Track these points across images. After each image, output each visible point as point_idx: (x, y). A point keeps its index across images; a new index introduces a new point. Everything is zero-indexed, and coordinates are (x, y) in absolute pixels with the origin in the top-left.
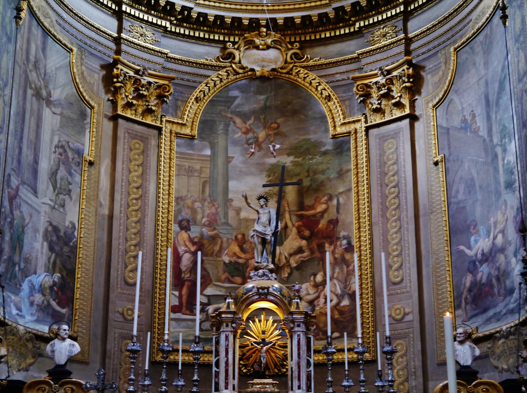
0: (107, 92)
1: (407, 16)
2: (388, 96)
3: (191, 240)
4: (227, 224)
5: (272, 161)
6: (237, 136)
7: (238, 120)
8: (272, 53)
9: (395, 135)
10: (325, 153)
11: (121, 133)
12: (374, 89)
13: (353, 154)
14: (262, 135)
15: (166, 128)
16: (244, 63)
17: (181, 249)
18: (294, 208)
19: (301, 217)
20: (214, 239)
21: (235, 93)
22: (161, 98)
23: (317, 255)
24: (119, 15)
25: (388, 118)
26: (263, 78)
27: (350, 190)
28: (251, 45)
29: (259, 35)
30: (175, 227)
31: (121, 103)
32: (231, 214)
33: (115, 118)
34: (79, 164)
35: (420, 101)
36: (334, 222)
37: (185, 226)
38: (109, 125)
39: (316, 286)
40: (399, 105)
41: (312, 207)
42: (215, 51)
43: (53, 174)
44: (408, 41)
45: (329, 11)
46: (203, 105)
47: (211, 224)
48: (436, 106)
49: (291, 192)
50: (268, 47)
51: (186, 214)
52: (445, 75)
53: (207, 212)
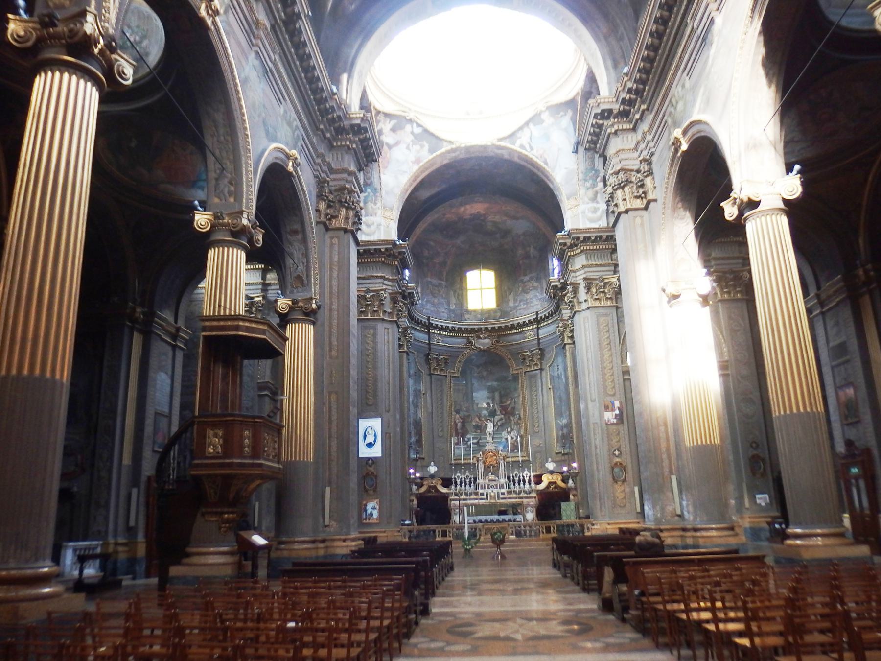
0: (427, 364)
1: (538, 328)
2: (532, 360)
3: (460, 417)
4: (473, 410)
5: (489, 384)
6: (476, 374)
7: (475, 368)
8: (487, 341)
9: (535, 376)
10: (509, 381)
11: (433, 380)
12: (527, 357)
13: (520, 381)
14: (485, 373)
15: (448, 375)
16: (476, 345)
17: (457, 421)
18: (498, 403)
19: (501, 406)
20: (469, 416)
21: (474, 357)
22: (446, 363)
23: (508, 421)
24: (429, 333)
25: (532, 369)
26: (484, 351)
27: (519, 396)
28: (479, 338)
29: (482, 334)
30: (454, 413)
31: (432, 368)
32: (475, 407)
33: (430, 374)
34: (420, 395)
35: (544, 363)
36: (514, 408)
37: (458, 412)
38: (428, 377)
39: (508, 433)
40: (536, 364)
41: (505, 402)
42: (465, 340)
43: (413, 401)
44: (539, 339)
45: (509, 324)
46: (462, 364)
47: (467, 411)
48: (549, 366)
49: (497, 395)
50: (485, 338)
51: (458, 408)
52: (552, 356)
53: (466, 405)
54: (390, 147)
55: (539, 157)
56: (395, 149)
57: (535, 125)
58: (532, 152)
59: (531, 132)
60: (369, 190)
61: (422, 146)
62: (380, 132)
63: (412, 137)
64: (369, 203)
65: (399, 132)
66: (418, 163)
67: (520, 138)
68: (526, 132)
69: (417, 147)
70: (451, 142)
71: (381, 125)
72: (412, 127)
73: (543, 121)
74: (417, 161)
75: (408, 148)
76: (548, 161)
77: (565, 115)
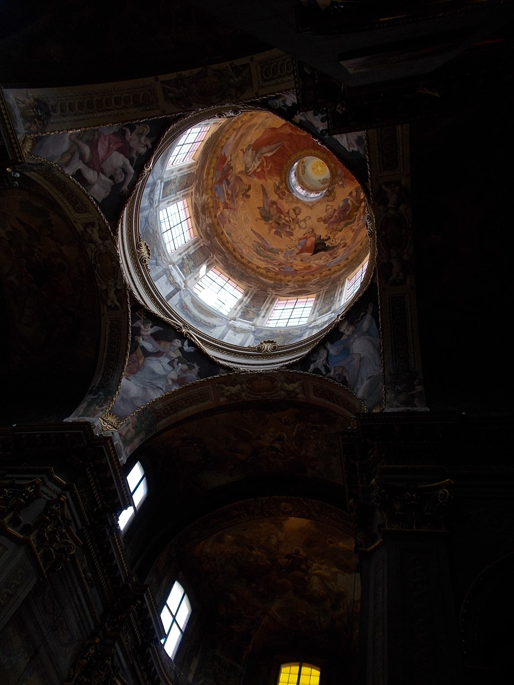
54: (146, 354)
55: (337, 378)
56: (153, 358)
57: (332, 343)
58: (328, 375)
59: (328, 351)
60: (101, 393)
61: (191, 368)
62: (137, 332)
63: (179, 354)
64: (95, 404)
65: (163, 343)
66: (180, 385)
67: (315, 361)
68: (323, 354)
69: (185, 367)
70: (229, 369)
71: (139, 323)
72: (183, 344)
73: (342, 334)
74: (179, 381)
75: (171, 363)
76: (347, 378)
77: (366, 313)
